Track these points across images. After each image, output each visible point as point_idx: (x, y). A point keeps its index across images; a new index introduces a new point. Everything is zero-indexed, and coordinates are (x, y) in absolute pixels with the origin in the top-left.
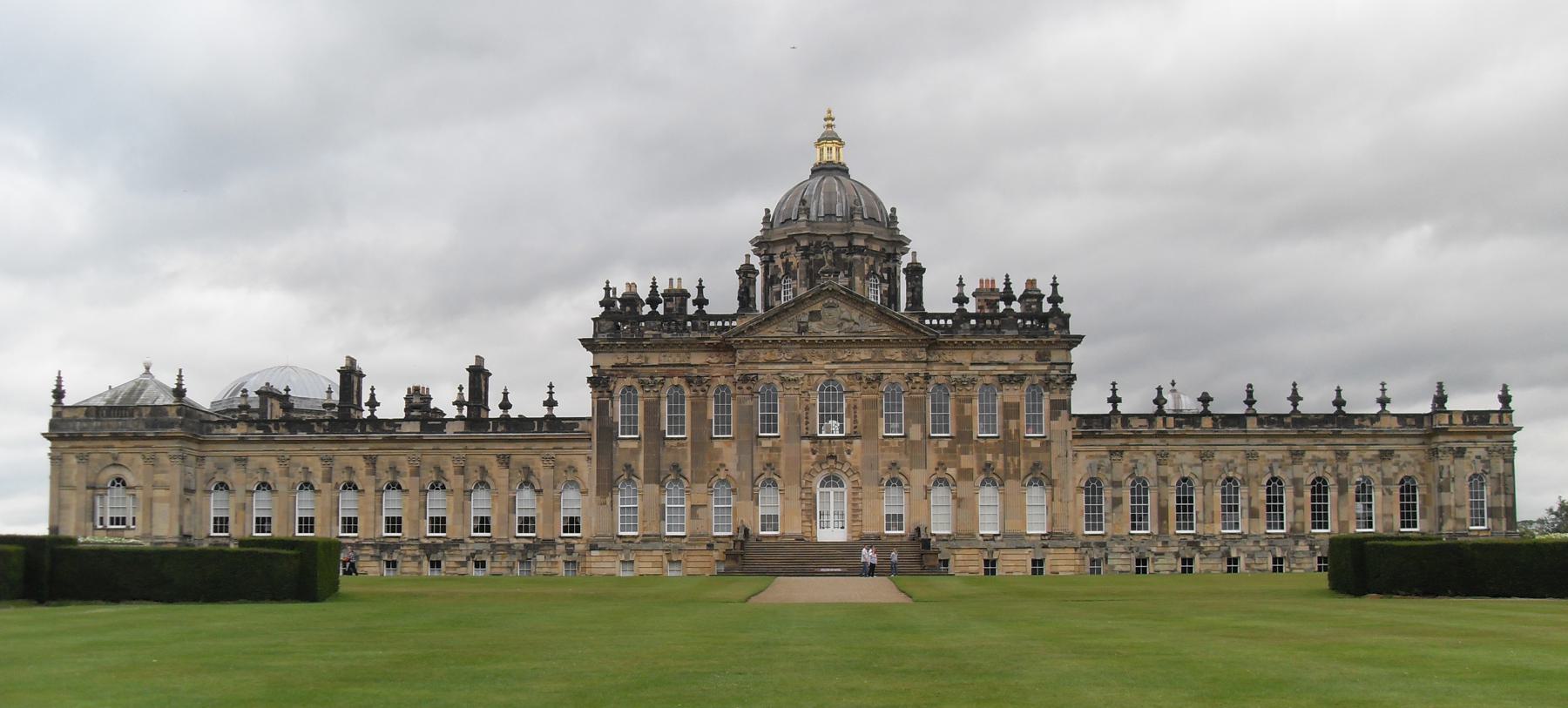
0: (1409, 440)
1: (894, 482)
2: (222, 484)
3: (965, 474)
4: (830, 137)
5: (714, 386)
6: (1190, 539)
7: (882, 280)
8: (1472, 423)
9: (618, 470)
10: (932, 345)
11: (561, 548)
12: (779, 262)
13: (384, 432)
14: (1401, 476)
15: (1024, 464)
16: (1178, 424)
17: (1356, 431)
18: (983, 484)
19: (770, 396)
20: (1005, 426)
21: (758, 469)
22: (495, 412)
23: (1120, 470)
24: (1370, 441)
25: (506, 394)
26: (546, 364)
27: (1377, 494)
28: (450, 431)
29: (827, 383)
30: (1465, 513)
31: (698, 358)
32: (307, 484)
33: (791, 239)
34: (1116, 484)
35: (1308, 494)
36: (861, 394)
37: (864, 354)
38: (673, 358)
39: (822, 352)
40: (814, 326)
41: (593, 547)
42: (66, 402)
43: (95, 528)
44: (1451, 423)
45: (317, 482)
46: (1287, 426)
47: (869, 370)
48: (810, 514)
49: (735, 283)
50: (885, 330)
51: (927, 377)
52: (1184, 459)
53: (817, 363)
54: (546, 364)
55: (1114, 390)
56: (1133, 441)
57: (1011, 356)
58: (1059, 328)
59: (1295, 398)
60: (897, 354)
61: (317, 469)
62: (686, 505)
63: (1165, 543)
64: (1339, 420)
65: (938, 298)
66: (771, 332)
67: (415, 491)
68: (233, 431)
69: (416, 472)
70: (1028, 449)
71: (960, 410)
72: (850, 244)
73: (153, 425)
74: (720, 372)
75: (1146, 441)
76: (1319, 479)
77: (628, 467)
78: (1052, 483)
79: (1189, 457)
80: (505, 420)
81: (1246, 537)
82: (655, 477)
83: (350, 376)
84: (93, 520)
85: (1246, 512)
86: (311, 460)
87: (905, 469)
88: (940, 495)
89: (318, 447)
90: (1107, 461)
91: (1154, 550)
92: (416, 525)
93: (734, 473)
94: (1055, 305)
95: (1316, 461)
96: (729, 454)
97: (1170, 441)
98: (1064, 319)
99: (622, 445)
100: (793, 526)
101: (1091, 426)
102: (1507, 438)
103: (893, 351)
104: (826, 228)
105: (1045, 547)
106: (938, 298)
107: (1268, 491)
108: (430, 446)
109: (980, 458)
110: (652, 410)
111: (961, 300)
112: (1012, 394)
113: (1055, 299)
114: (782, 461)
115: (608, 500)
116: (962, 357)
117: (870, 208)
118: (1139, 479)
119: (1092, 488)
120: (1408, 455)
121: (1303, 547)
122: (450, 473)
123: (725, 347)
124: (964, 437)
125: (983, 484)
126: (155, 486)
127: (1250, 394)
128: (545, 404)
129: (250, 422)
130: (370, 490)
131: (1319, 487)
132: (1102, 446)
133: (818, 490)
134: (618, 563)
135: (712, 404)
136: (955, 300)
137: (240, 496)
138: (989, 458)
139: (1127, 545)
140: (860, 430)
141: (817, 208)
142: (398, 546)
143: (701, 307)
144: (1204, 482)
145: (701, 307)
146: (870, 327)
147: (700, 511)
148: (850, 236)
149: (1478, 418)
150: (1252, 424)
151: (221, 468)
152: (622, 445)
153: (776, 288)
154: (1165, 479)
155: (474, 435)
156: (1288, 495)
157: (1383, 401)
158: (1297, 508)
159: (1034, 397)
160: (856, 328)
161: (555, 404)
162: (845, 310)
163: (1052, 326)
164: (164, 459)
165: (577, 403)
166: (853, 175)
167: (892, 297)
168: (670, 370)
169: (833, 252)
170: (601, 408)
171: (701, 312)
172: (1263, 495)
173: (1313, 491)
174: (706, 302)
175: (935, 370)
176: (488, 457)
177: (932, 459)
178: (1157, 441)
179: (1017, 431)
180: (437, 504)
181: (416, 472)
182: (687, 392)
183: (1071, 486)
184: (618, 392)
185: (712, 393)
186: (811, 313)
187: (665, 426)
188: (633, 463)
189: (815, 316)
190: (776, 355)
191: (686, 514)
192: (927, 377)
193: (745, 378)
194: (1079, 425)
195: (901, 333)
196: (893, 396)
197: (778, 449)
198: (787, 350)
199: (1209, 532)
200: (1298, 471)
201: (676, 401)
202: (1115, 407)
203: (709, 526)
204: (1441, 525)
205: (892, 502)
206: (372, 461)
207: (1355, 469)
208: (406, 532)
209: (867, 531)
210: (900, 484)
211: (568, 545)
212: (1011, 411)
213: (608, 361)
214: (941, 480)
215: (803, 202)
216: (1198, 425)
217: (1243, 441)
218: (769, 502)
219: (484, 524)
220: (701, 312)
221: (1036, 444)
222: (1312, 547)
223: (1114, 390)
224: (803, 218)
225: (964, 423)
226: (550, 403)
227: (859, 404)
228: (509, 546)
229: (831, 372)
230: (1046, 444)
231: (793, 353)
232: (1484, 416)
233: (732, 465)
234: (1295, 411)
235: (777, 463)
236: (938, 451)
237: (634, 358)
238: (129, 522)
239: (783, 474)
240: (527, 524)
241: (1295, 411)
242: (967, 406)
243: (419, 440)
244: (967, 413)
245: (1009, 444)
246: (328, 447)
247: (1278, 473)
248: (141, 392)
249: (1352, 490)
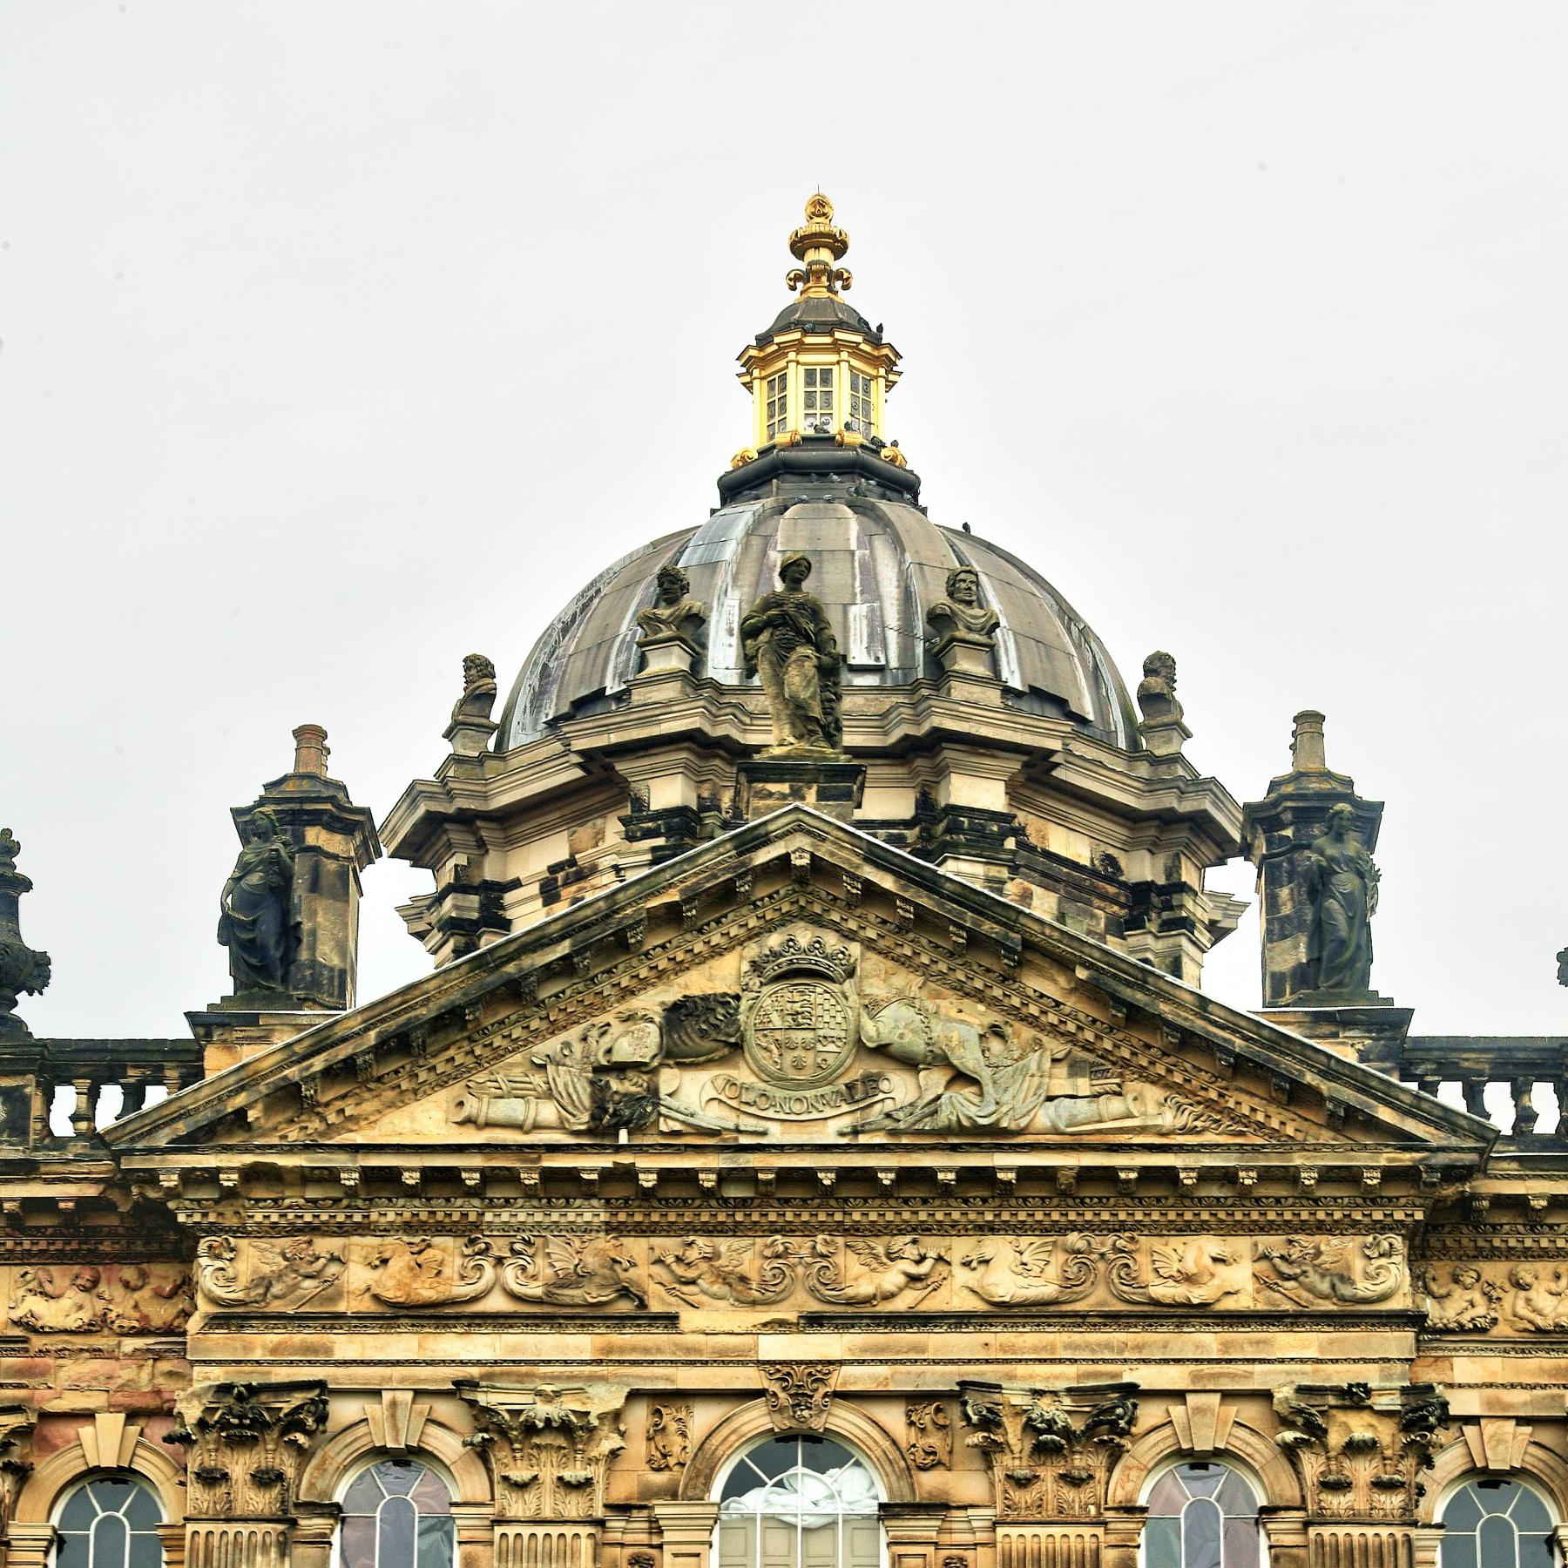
4: (820, 320)
5: (53, 1470)
39: (745, 1255)
53: (712, 1320)
72: (927, 808)
103: (1198, 1250)
123: (130, 1231)
146: (1047, 1098)
148: (924, 754)
160: (962, 1106)
162: (893, 999)
166: (943, 502)
175: (1467, 1378)
186: (679, 1013)
189: (700, 1031)
190: (449, 1269)
192: (1423, 1415)
193: (245, 1416)
198: (525, 1242)
215: (671, 585)
229: (800, 1382)
231: (560, 1256)
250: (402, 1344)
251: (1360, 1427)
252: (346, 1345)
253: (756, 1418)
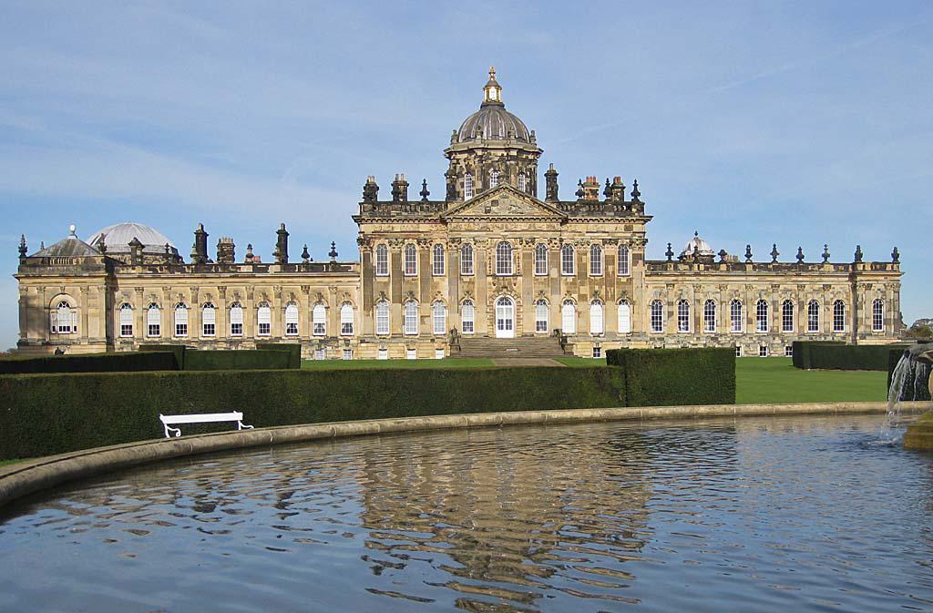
0: (840, 279)
1: (541, 302)
2: (126, 304)
3: (583, 298)
5: (433, 244)
6: (713, 336)
7: (527, 176)
8: (876, 270)
9: (376, 295)
10: (565, 221)
11: (341, 342)
12: (463, 164)
13: (230, 272)
14: (835, 300)
15: (617, 291)
16: (707, 269)
17: (809, 273)
18: (593, 303)
19: (467, 251)
20: (606, 269)
21: (461, 294)
22: (294, 257)
24: (817, 279)
25: (305, 249)
27: (821, 310)
28: (272, 270)
29: (502, 243)
30: (871, 322)
31: (424, 227)
32: (181, 304)
33: (471, 151)
34: (670, 304)
35: (781, 310)
36: (521, 250)
37: (523, 226)
38: (409, 227)
40: (494, 208)
41: (362, 342)
42: (27, 254)
43: (50, 333)
44: (864, 270)
45: (188, 303)
46: (770, 270)
47: (527, 236)
48: (492, 324)
49: (444, 182)
50: (537, 211)
51: (561, 240)
52: (709, 286)
53: (496, 231)
55: (669, 248)
56: (680, 278)
57: (610, 227)
58: (638, 211)
59: (775, 253)
60: (544, 226)
61: (189, 294)
62: (418, 316)
63: (698, 338)
64: (800, 267)
65: (567, 193)
66: (468, 212)
67: (250, 308)
68: (133, 271)
69: (251, 297)
70: (619, 283)
71: (580, 259)
73: (87, 270)
74: (438, 234)
75: (687, 278)
76: (788, 301)
77: (383, 293)
78: (633, 303)
79: (713, 288)
80: (306, 265)
81: (745, 335)
82: (399, 299)
83: (202, 237)
84: (49, 328)
85: (745, 321)
86: (183, 286)
87: (549, 295)
88: (568, 309)
89: (188, 281)
90: (665, 290)
91: (692, 342)
92: (252, 328)
93: (446, 297)
94: (636, 197)
95: (786, 291)
96: (444, 285)
97: (701, 278)
98: (641, 208)
99: (378, 280)
100: (481, 328)
101: (656, 268)
102: (897, 278)
103: (541, 224)
104: (493, 144)
105: (629, 340)
106: (567, 193)
107: (758, 308)
108: (260, 280)
109: (591, 288)
110: (396, 258)
111: (580, 194)
112: (611, 250)
113: (636, 194)
114: (476, 290)
115: (371, 313)
116: (581, 227)
117: (519, 131)
118: (683, 301)
119: (656, 307)
120: (841, 286)
121: (778, 341)
122: (272, 297)
124: (582, 275)
125: (593, 303)
126: (89, 306)
127: (748, 251)
128: (330, 255)
129: (144, 267)
130: (223, 307)
131: (788, 306)
132: (662, 281)
133: (497, 307)
134: (377, 351)
135: (432, 255)
136: (576, 194)
137: (139, 312)
138: (597, 288)
139: (676, 339)
140: (521, 271)
142: (241, 342)
143: (425, 196)
144: (721, 303)
145: (425, 196)
147: (426, 319)
149: (879, 267)
150: (749, 267)
151: (127, 295)
152: (378, 280)
153: (461, 180)
154: (699, 301)
155: (287, 274)
156: (770, 310)
157: (826, 256)
158: (774, 318)
159: (623, 253)
161: (337, 255)
162: (513, 199)
163: (634, 210)
164: (94, 289)
165: (350, 253)
167: (532, 187)
168: (408, 235)
169: (496, 156)
170: (366, 258)
171: (425, 199)
172: (755, 310)
173: (784, 308)
174: (428, 194)
175: (565, 236)
176: (295, 284)
177: (564, 288)
178: (694, 278)
179: (613, 272)
180: (265, 315)
181: (251, 297)
182: (417, 248)
183: (645, 307)
184: (375, 249)
185: (432, 249)
186: (492, 201)
187: (404, 268)
188: (385, 291)
189: (495, 203)
191: (418, 321)
192: (561, 240)
194: (649, 268)
195: (546, 213)
196: (541, 251)
197: (473, 283)
199: (723, 332)
200: (775, 296)
201: (411, 254)
202: (670, 258)
203: (431, 328)
204: (857, 331)
205: (541, 314)
206: (223, 290)
207: (809, 295)
208: (245, 333)
209: (526, 331)
210: (545, 303)
211: (345, 340)
212: (609, 260)
213: (368, 228)
214: (568, 301)
216: (718, 269)
217: (744, 278)
218: (469, 315)
219: (292, 329)
220: (425, 199)
221: (624, 280)
222: (783, 341)
223: (669, 248)
224: (479, 137)
225: (582, 266)
226: (333, 254)
227: (521, 256)
228: (310, 341)
229: (504, 237)
230: (630, 280)
231: (481, 225)
232: (883, 266)
233: (445, 293)
234: (774, 261)
235: (472, 291)
236: (567, 284)
237: (385, 227)
238: (72, 329)
239: (476, 297)
240: (320, 328)
241: (774, 261)
242: (584, 257)
243: (254, 277)
244: (584, 261)
245: (609, 281)
246: (195, 281)
247: (764, 298)
248: (72, 247)
249: (807, 308)
250: (468, 233)
251: (554, 241)
252: (462, 233)
253: (500, 240)
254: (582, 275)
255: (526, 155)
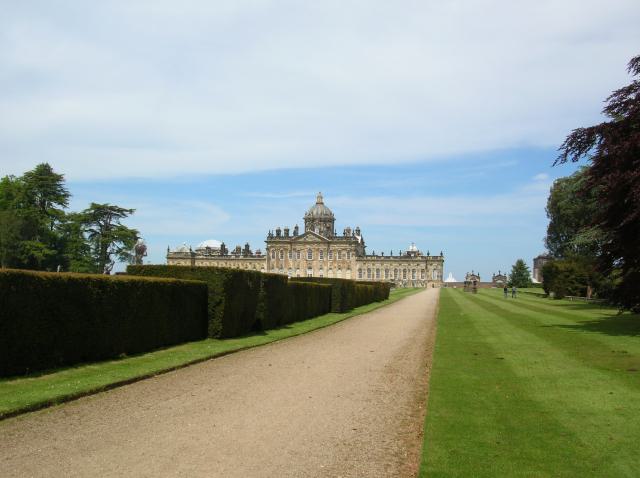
15: (346, 265)
23: (365, 267)
26: (259, 245)
54: (259, 245)
112: (344, 252)
119: (360, 270)
123: (290, 243)
124: (335, 260)
132: (362, 263)
141: (315, 213)
212: (344, 255)
245: (344, 262)
254: (335, 260)
255: (328, 220)
